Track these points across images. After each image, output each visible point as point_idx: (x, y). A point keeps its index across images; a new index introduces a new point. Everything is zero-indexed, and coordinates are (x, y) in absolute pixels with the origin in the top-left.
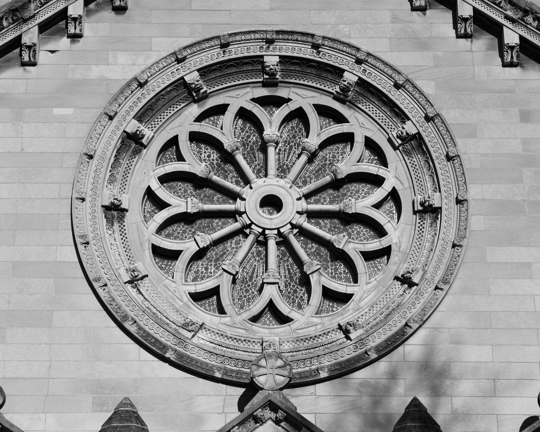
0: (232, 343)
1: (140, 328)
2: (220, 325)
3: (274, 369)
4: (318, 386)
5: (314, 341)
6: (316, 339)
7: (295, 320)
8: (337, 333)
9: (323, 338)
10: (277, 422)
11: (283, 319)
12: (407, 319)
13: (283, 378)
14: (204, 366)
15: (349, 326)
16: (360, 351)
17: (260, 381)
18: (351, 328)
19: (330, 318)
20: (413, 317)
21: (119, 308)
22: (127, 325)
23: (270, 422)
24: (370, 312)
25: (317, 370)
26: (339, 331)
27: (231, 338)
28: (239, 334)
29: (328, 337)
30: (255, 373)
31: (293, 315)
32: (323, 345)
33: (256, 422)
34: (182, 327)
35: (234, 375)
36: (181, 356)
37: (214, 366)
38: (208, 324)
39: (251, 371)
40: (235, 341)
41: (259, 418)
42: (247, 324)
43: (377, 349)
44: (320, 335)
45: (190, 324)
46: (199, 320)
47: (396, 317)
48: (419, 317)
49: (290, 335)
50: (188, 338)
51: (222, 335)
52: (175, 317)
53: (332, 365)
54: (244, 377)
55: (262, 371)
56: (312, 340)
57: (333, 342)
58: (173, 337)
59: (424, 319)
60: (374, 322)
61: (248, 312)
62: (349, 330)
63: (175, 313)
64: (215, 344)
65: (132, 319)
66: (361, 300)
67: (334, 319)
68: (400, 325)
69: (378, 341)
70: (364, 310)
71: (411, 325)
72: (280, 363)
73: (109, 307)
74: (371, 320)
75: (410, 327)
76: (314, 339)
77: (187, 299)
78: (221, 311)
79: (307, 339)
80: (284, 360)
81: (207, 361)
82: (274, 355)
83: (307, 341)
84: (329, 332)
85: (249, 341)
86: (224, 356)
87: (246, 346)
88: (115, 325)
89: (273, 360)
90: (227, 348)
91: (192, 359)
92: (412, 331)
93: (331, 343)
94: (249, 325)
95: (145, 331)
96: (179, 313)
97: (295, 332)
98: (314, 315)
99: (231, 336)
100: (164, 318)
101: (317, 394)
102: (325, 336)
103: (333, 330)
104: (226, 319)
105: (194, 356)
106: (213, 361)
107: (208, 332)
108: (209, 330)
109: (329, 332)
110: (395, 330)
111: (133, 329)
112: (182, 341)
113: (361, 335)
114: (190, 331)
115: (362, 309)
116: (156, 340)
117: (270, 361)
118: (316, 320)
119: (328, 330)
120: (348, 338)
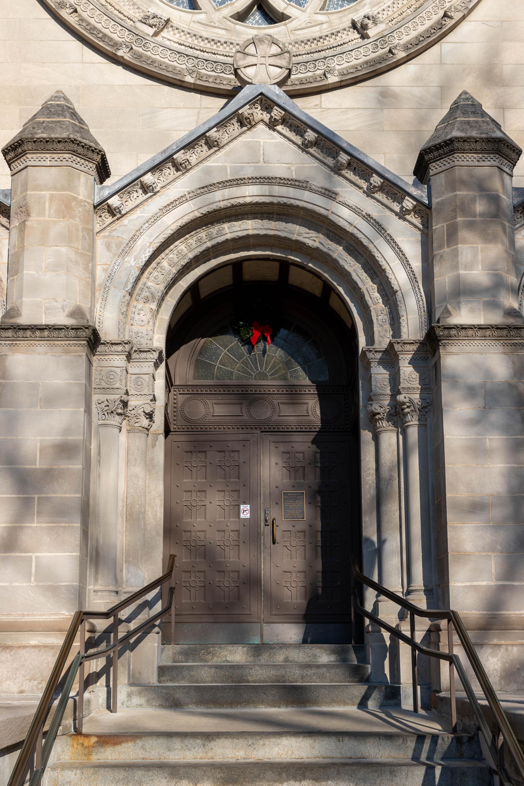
0: (208, 45)
1: (82, 20)
2: (192, 24)
3: (267, 58)
4: (324, 96)
5: (319, 43)
6: (321, 40)
7: (293, 17)
8: (349, 33)
9: (331, 40)
10: (272, 125)
12: (445, 9)
13: (279, 70)
14: (170, 69)
15: (366, 21)
17: (248, 73)
18: (370, 23)
19: (339, 15)
20: (455, 5)
22: (64, 13)
23: (261, 127)
24: (394, 5)
25: (324, 75)
26: (352, 30)
27: (207, 39)
28: (218, 36)
29: (337, 38)
30: (241, 63)
31: (291, 10)
32: (331, 48)
33: (242, 125)
34: (141, 21)
35: (211, 80)
36: (139, 57)
37: (184, 69)
38: (175, 22)
39: (235, 60)
40: (213, 43)
41: (247, 118)
42: (228, 22)
43: (406, 48)
44: (327, 36)
45: (151, 17)
46: (164, 15)
48: (463, 5)
49: (286, 37)
50: (148, 35)
51: (195, 35)
52: (131, 12)
53: (342, 69)
54: (225, 83)
55: (250, 60)
56: (315, 42)
57: (344, 43)
58: (127, 32)
59: (470, 6)
60: (401, 18)
61: (230, 7)
62: (367, 25)
63: (132, 7)
64: (186, 46)
65: (71, 6)
67: (345, 16)
68: (436, 18)
69: (405, 39)
70: (385, 4)
71: (452, 14)
72: (275, 50)
74: (396, 15)
75: (451, 18)
76: (318, 41)
79: (309, 40)
80: (281, 46)
81: (175, 64)
82: (266, 39)
83: (309, 43)
84: (339, 32)
85: (232, 43)
86: (197, 58)
87: (228, 49)
88: (48, 16)
89: (265, 46)
90: (201, 51)
91: (153, 62)
92: (453, 22)
93: (341, 45)
94: (231, 24)
95: (89, 24)
96: (136, 7)
97: (294, 34)
98: (318, 11)
99: (207, 37)
100: (116, 12)
101: (323, 106)
102: (333, 37)
103: (345, 30)
104: (200, 17)
105: (158, 57)
106: (181, 65)
107: (176, 31)
108: (177, 29)
109: (339, 32)
110: (428, 24)
111: (72, 20)
112: (140, 38)
113: (383, 31)
114: (151, 26)
115: (383, 4)
116: (105, 35)
117: (261, 47)
118: (321, 18)
119: (337, 30)
120: (364, 36)
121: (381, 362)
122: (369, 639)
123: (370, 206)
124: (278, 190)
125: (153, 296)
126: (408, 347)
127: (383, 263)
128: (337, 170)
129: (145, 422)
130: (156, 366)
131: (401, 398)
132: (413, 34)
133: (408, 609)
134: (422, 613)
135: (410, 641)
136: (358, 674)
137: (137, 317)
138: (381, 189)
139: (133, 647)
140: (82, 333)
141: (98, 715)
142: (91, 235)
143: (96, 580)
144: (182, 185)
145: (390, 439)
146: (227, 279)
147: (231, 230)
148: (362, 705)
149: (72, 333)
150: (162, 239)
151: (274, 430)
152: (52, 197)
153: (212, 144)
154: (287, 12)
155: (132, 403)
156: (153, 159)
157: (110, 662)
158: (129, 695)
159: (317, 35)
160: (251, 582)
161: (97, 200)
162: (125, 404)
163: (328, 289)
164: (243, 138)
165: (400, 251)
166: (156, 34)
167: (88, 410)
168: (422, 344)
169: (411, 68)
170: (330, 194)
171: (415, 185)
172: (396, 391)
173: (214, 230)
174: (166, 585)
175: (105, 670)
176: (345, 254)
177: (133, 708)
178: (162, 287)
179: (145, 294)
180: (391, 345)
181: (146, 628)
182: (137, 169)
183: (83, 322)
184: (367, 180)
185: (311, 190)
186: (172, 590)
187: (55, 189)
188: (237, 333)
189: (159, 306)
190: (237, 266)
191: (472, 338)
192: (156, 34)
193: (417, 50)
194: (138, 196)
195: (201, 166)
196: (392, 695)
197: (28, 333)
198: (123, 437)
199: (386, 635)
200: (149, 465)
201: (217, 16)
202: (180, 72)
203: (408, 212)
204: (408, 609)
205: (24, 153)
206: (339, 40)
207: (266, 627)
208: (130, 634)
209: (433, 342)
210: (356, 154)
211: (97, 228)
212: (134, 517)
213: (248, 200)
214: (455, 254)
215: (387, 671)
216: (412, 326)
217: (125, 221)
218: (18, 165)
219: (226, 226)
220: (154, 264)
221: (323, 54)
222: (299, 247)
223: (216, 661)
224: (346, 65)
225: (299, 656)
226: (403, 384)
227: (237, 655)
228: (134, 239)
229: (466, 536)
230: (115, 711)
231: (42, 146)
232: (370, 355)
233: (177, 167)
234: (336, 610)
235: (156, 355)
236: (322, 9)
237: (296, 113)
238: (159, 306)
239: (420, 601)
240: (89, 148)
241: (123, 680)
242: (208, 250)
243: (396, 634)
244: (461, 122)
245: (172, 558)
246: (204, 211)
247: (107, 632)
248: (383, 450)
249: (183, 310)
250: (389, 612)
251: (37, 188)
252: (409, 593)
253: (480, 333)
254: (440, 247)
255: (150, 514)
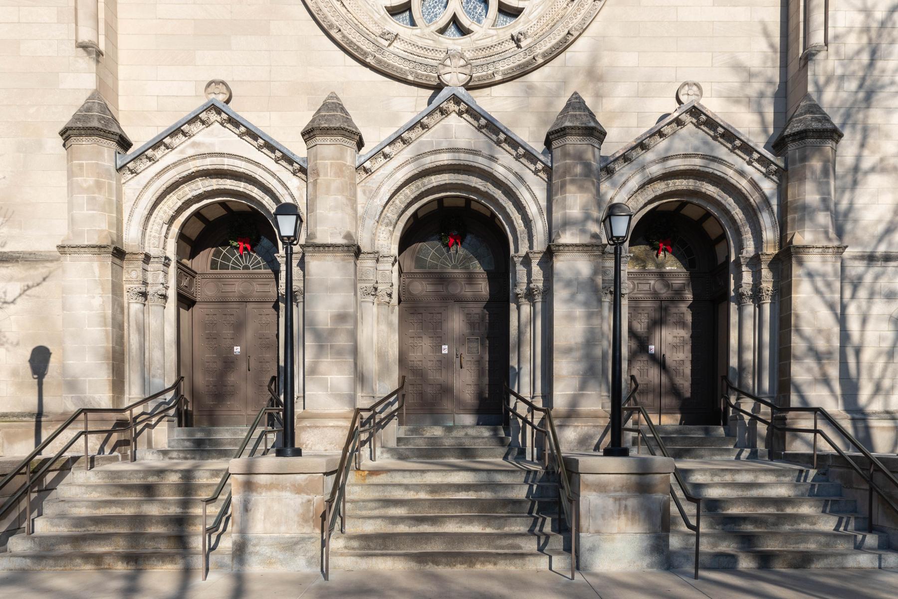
1: (344, 36)
10: (460, 114)
11: (464, 31)
16: (528, 58)
17: (446, 78)
18: (521, 37)
21: (326, 17)
22: (333, 33)
23: (454, 114)
30: (442, 71)
31: (473, 27)
33: (442, 114)
36: (380, 62)
38: (401, 35)
43: (544, 56)
47: (560, 26)
55: (447, 69)
66: (530, 13)
69: (544, 49)
73: (317, 16)
77: (384, 13)
78: (413, 23)
91: (389, 65)
92: (573, 38)
95: (348, 39)
104: (417, 31)
106: (406, 67)
110: (558, 38)
111: (338, 37)
112: (380, 48)
116: (358, 47)
118: (493, 32)
120: (519, 46)
121: (522, 263)
122: (511, 423)
123: (516, 166)
124: (463, 156)
125: (391, 222)
126: (537, 255)
127: (524, 202)
128: (498, 143)
129: (387, 299)
130: (393, 265)
131: (532, 285)
132: (549, 45)
133: (532, 408)
134: (538, 409)
135: (531, 424)
136: (502, 442)
137: (381, 235)
138: (524, 156)
139: (383, 427)
140: (352, 249)
141: (366, 462)
142: (354, 186)
143: (362, 390)
144: (407, 153)
145: (526, 309)
146: (435, 206)
147: (435, 180)
148: (505, 458)
149: (346, 248)
150: (395, 188)
151: (459, 300)
152: (332, 164)
153: (424, 127)
154: (471, 28)
155: (380, 288)
156: (390, 138)
157: (371, 435)
158: (382, 453)
159: (490, 44)
160: (446, 390)
161: (357, 164)
162: (376, 289)
163: (493, 216)
164: (443, 122)
165: (533, 193)
166: (390, 45)
167: (356, 294)
168: (545, 253)
169: (546, 69)
170: (492, 158)
171: (543, 153)
172: (529, 282)
173: (425, 180)
174: (400, 393)
175: (369, 439)
176: (503, 196)
177: (383, 460)
178: (395, 217)
179: (386, 221)
180: (527, 253)
181: (390, 417)
182: (381, 144)
183: (351, 242)
184: (516, 150)
185: (483, 156)
186: (404, 396)
187: (333, 159)
188: (440, 239)
189: (394, 227)
190: (440, 200)
191: (572, 251)
192: (390, 45)
193: (550, 56)
194: (381, 161)
195: (418, 140)
196: (522, 452)
197: (321, 249)
198: (375, 309)
199: (520, 421)
200: (390, 324)
201: (427, 31)
202: (405, 73)
203: (539, 171)
204: (532, 408)
205: (314, 136)
206: (503, 48)
207: (456, 416)
208: (382, 420)
209: (549, 254)
210: (509, 134)
211: (358, 181)
212: (382, 356)
213: (446, 162)
214: (565, 199)
215: (520, 441)
216: (540, 244)
217: (374, 176)
218: (312, 143)
219: (433, 178)
220: (391, 202)
221: (493, 59)
222: (476, 190)
223: (428, 435)
224: (507, 67)
225: (472, 432)
226: (534, 277)
227: (438, 432)
228: (379, 188)
229: (563, 367)
230: (375, 460)
231: (325, 131)
232: (516, 259)
233: (404, 142)
234: (494, 406)
235: (393, 259)
236: (493, 26)
237: (474, 107)
238: (394, 227)
239: (539, 403)
240: (352, 132)
241: (378, 445)
242: (422, 193)
243: (525, 420)
244: (572, 116)
245: (404, 377)
246: (420, 169)
247: (369, 419)
248: (521, 315)
249: (408, 226)
250: (522, 409)
251: (323, 158)
252: (533, 397)
253: (576, 249)
254: (556, 195)
255: (391, 352)
